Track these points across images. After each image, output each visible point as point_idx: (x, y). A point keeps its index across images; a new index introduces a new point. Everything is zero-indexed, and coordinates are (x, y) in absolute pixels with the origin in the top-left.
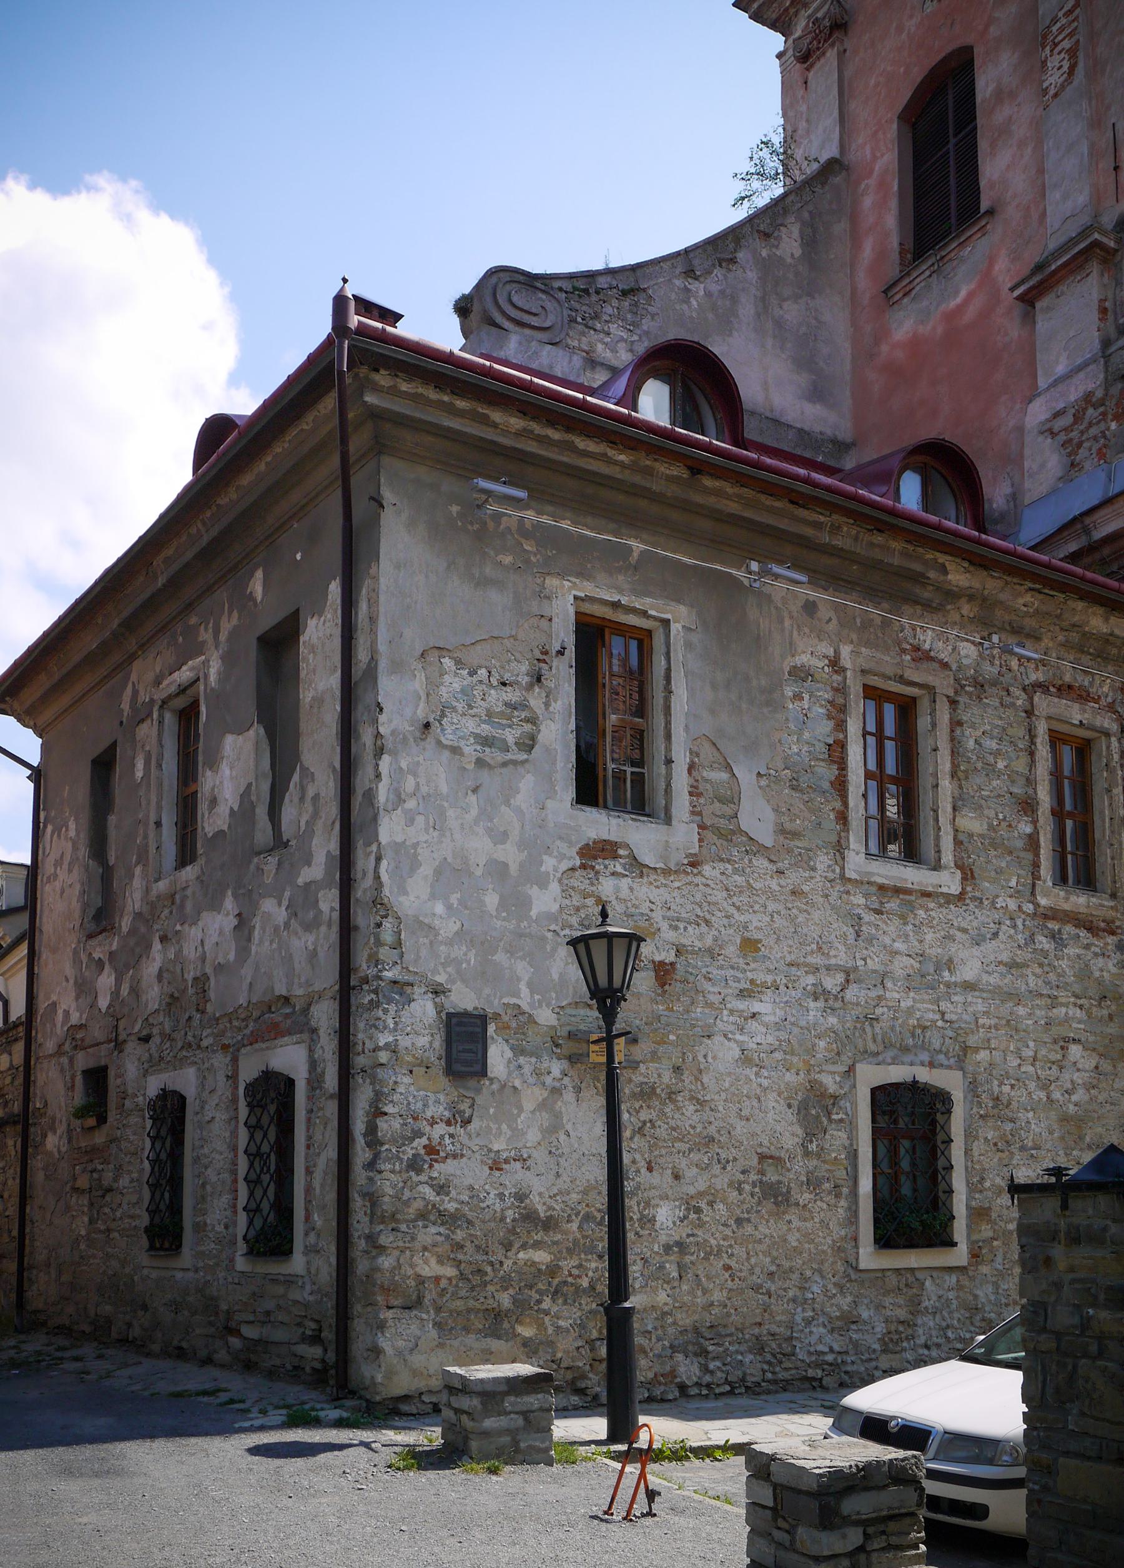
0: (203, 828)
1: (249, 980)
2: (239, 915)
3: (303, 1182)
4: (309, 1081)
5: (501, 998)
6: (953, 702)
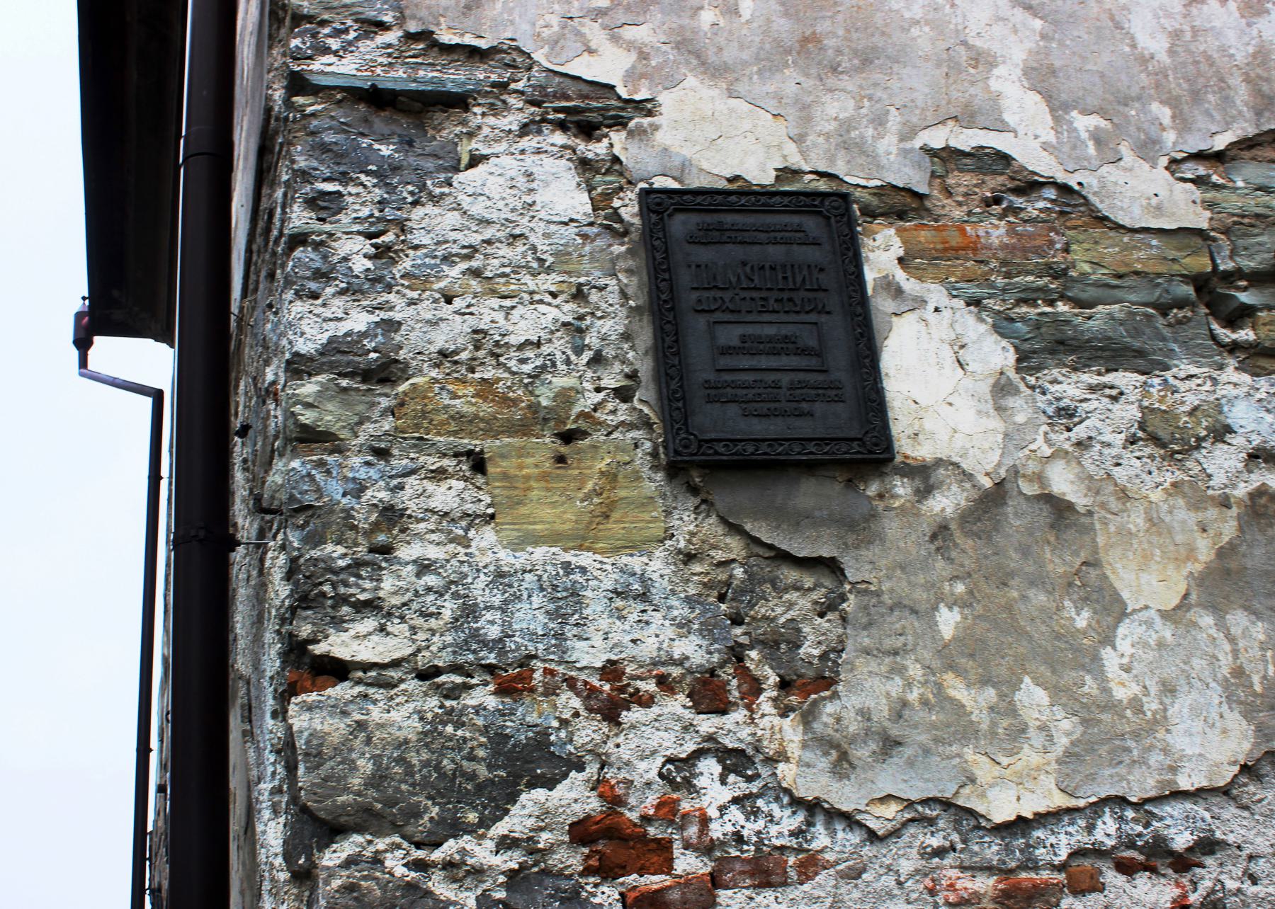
5: (908, 133)
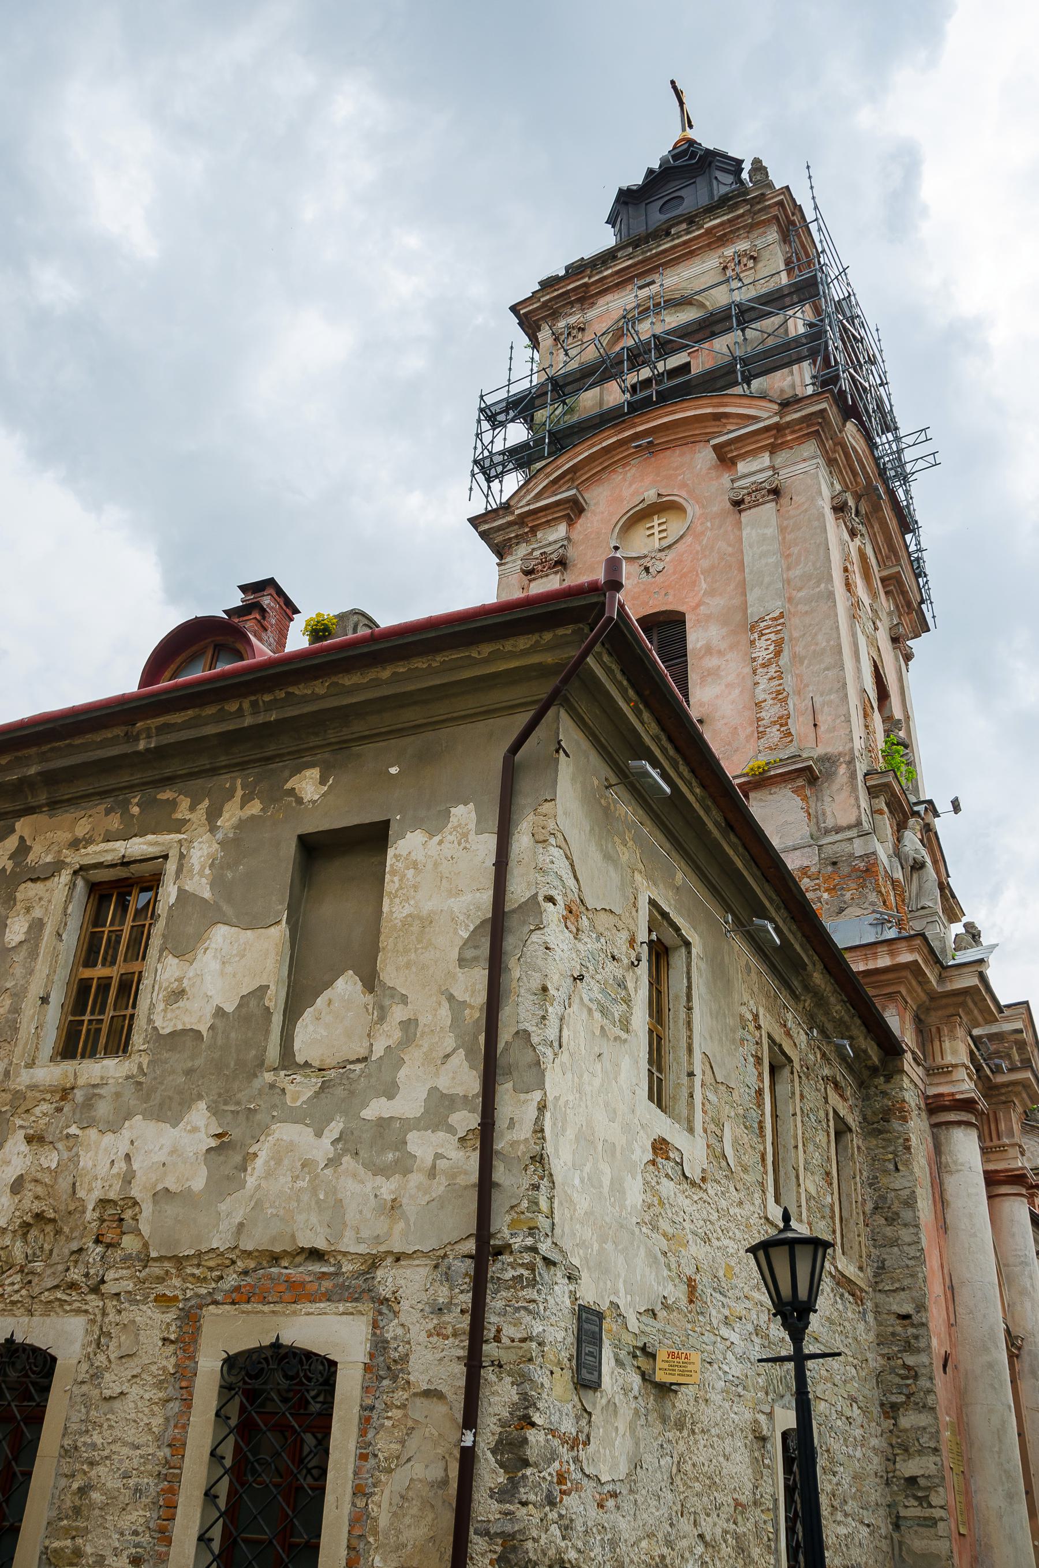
0: (150, 1021)
1: (238, 1220)
2: (218, 1136)
3: (347, 1508)
4: (367, 1368)
6: (800, 1077)
